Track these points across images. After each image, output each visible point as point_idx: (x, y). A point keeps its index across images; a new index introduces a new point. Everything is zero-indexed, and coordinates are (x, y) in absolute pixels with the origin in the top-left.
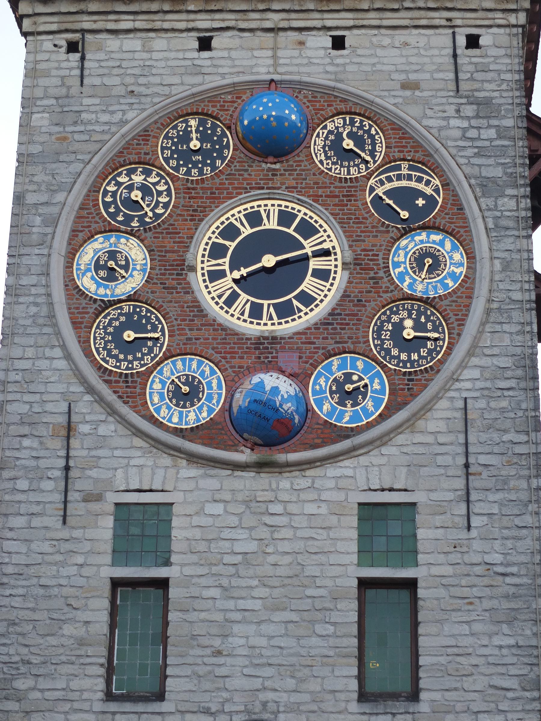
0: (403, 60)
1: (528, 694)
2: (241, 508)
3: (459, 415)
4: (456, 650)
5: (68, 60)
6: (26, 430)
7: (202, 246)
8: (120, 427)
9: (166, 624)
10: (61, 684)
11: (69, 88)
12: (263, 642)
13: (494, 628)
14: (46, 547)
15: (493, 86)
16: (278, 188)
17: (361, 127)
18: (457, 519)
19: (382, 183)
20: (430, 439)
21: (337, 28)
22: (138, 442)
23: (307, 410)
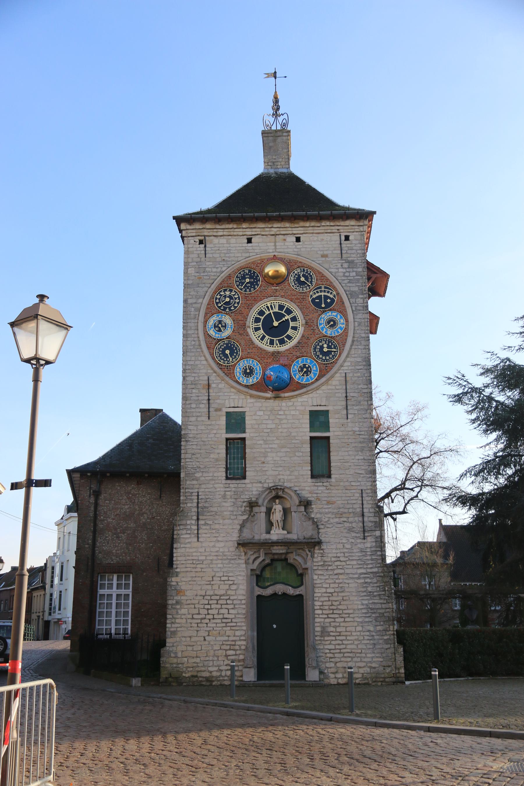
0: (322, 246)
1: (368, 476)
2: (269, 413)
3: (344, 379)
4: (343, 461)
5: (200, 247)
6: (193, 386)
7: (252, 318)
8: (226, 385)
9: (245, 453)
10: (211, 475)
11: (201, 258)
12: (278, 459)
13: (356, 453)
14: (203, 428)
15: (354, 256)
16: (278, 296)
17: (307, 272)
18: (343, 416)
19: (315, 294)
20: (334, 387)
21: (297, 234)
22: (233, 390)
23: (291, 378)
